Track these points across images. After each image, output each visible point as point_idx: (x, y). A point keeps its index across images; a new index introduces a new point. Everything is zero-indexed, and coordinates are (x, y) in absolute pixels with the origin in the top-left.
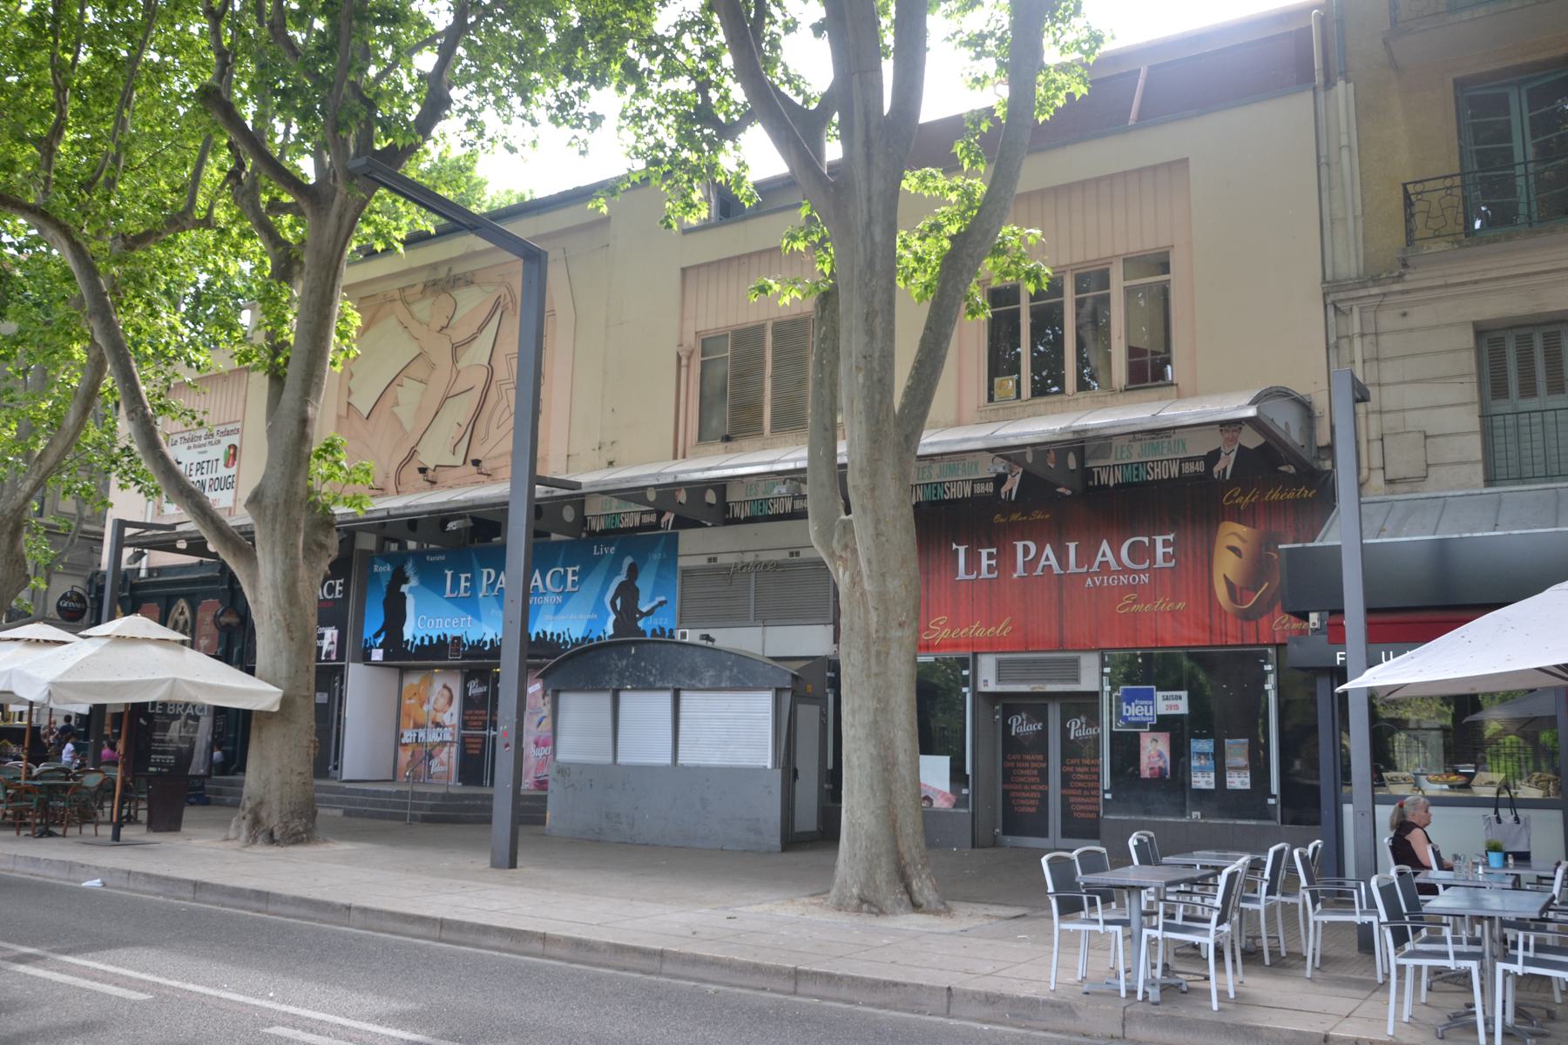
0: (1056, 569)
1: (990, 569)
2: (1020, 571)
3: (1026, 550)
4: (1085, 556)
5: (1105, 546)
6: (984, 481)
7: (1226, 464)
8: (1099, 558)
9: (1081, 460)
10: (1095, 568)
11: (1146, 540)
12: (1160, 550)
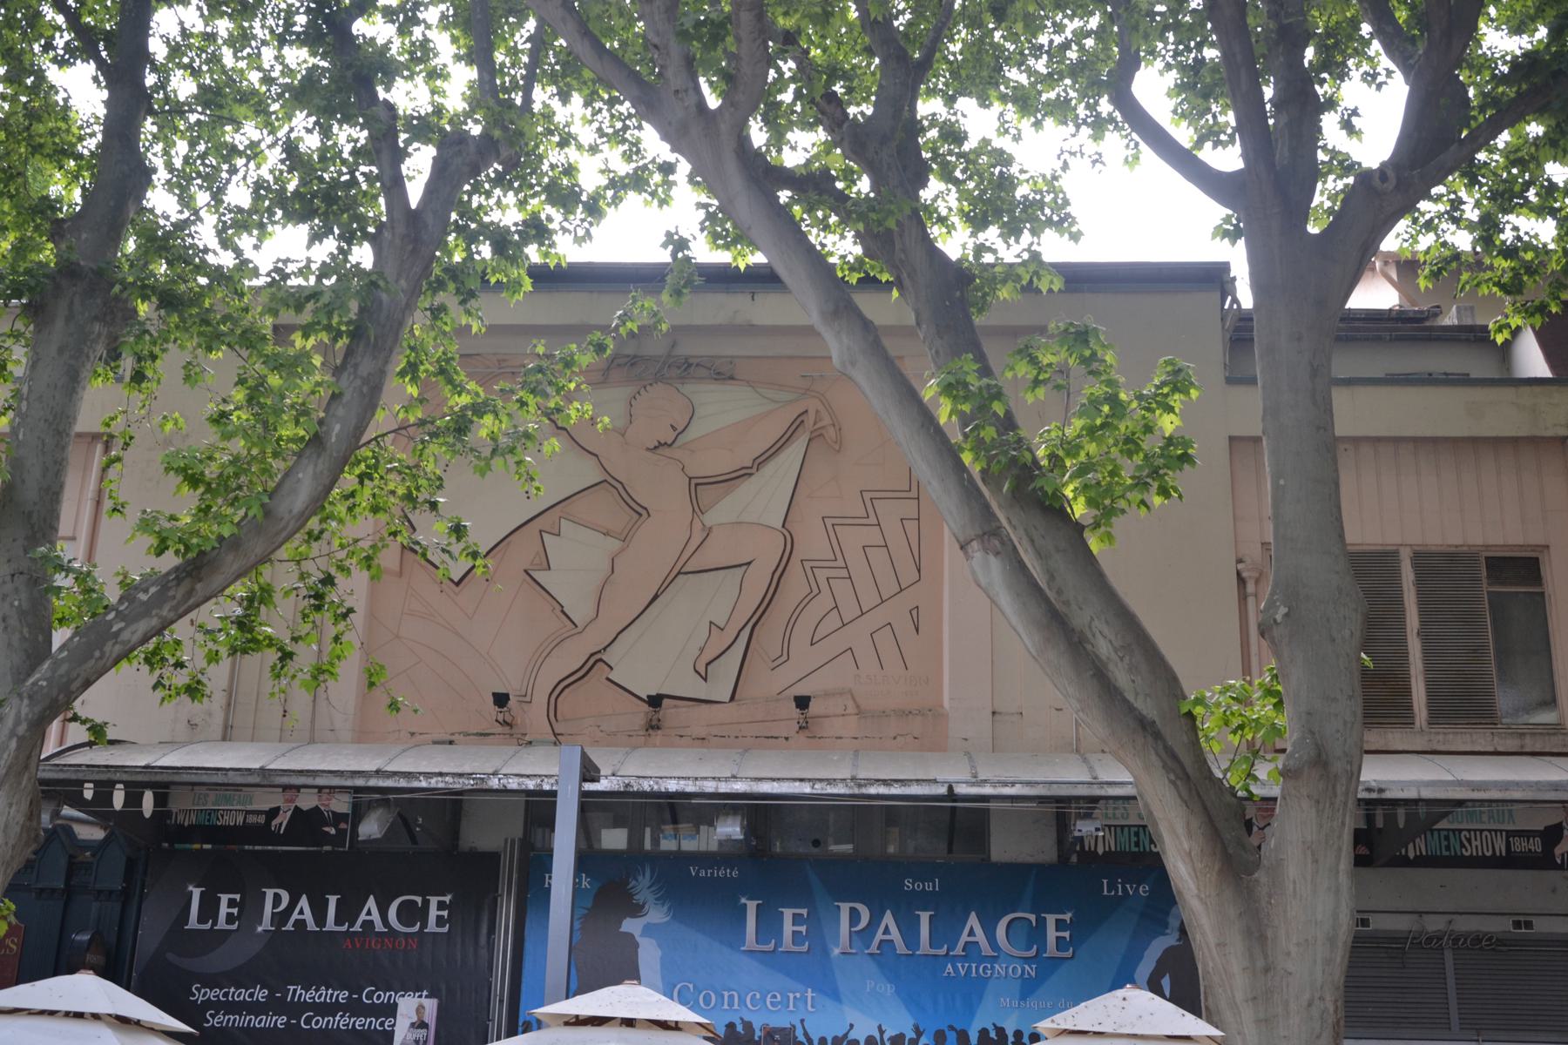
0: (311, 925)
1: (230, 918)
2: (266, 924)
3: (277, 899)
4: (347, 912)
5: (973, 921)
6: (258, 813)
7: (283, 820)
8: (964, 937)
9: (160, 800)
10: (958, 950)
11: (419, 899)
12: (433, 912)
